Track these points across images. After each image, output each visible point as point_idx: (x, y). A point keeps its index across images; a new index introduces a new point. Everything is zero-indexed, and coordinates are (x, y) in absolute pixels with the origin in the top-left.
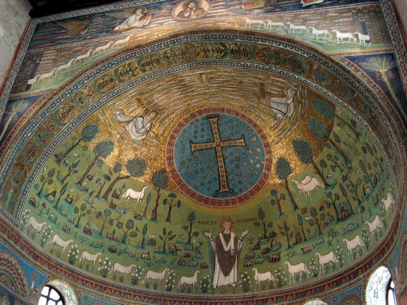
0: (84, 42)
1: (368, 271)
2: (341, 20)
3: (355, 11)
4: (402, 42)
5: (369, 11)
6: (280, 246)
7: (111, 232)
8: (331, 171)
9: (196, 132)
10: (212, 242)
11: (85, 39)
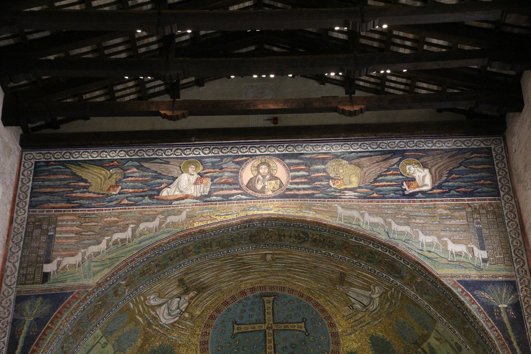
0: (118, 210)
2: (453, 222)
3: (469, 210)
4: (526, 267)
5: (488, 212)
11: (119, 205)
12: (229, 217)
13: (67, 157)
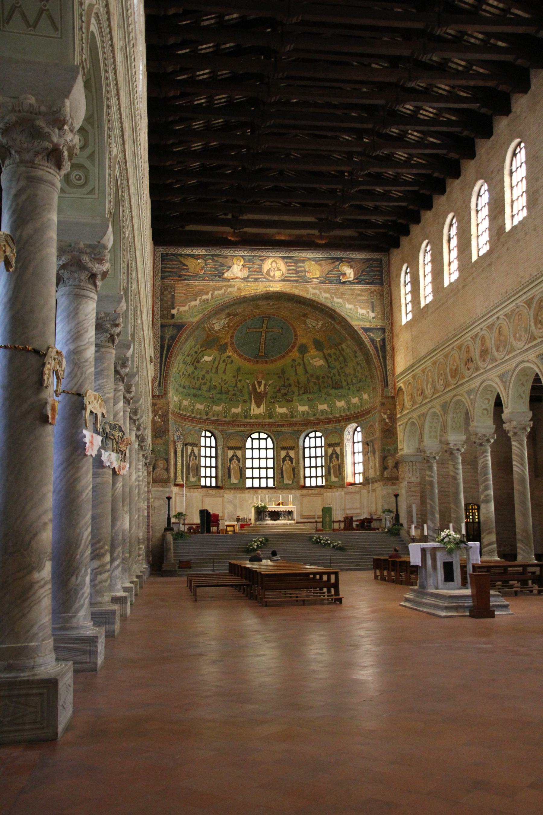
0: (204, 283)
2: (362, 298)
3: (369, 292)
5: (377, 293)
7: (194, 384)
8: (334, 361)
9: (252, 323)
11: (204, 280)
12: (259, 291)
13: (176, 252)
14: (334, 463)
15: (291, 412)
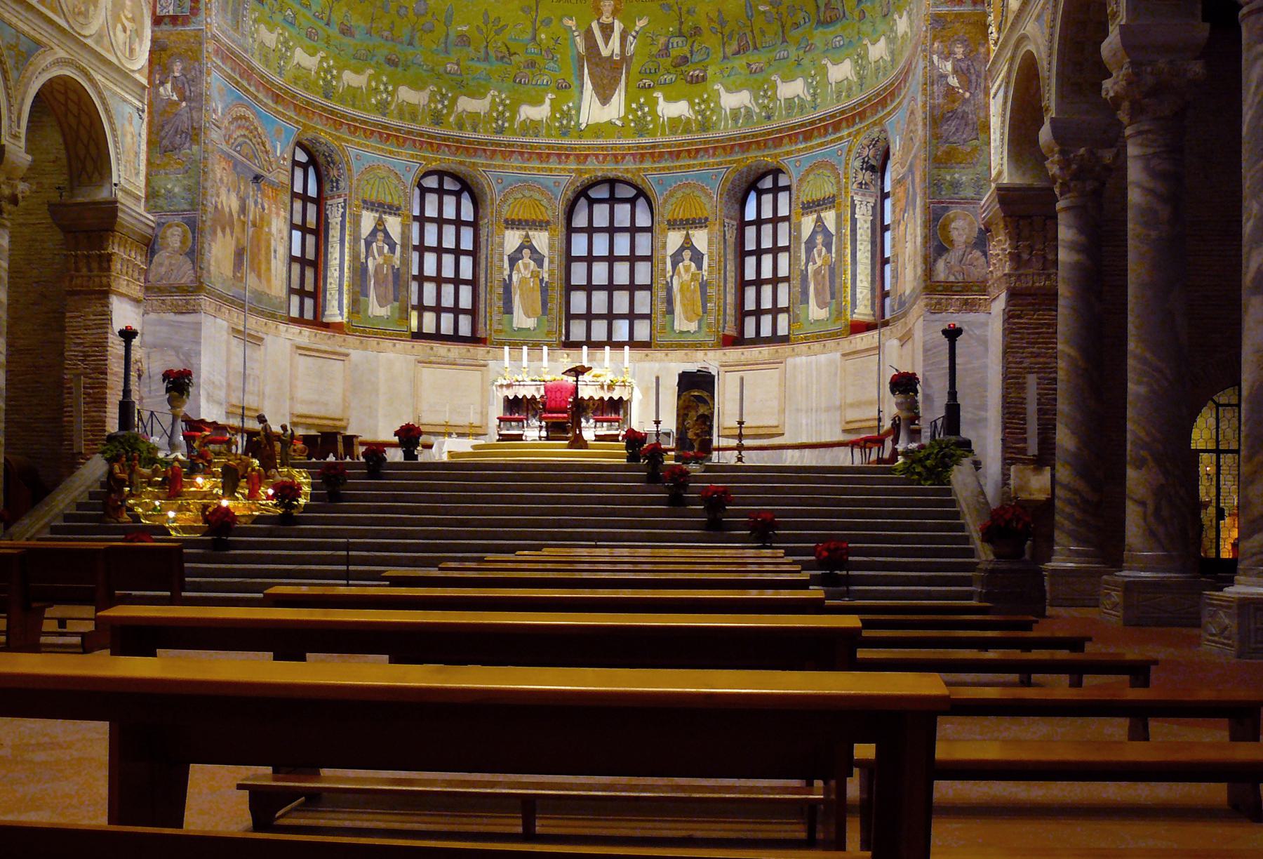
1: (856, 127)
6: (708, 55)
10: (578, 39)
14: (819, 263)
15: (702, 112)
